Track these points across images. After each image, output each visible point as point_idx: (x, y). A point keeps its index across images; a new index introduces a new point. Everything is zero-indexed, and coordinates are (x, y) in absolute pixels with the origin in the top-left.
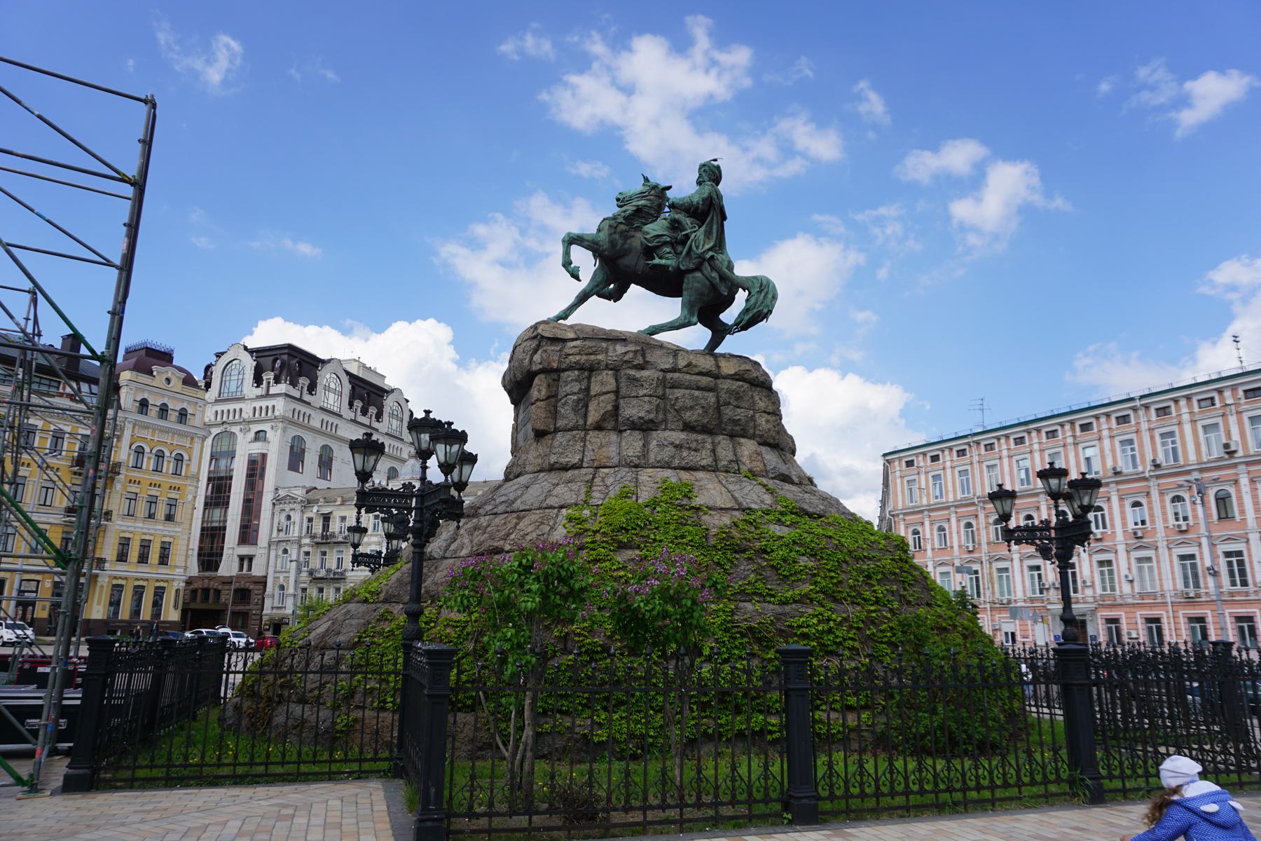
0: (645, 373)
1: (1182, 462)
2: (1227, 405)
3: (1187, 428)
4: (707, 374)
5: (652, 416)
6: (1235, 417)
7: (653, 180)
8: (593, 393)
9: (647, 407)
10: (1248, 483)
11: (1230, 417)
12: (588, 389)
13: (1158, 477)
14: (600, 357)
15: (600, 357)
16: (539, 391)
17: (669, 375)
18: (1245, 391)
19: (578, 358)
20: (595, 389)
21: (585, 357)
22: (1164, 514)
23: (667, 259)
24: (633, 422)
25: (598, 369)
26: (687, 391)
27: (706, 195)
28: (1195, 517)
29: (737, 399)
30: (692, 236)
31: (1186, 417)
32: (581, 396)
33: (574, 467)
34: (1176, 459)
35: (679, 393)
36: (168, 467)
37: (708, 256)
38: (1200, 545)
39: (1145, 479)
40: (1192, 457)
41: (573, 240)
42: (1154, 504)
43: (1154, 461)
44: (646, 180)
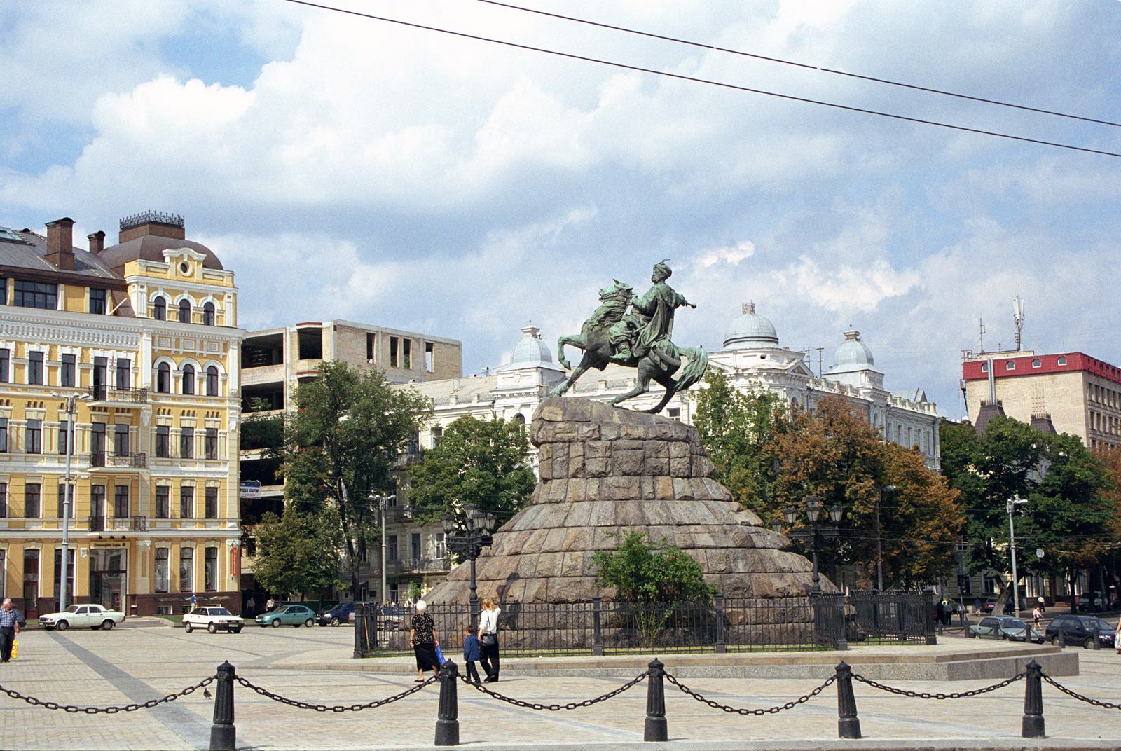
0: (599, 443)
4: (639, 438)
5: (603, 469)
9: (600, 464)
12: (568, 454)
14: (575, 434)
15: (575, 434)
17: (614, 443)
19: (562, 435)
20: (571, 455)
25: (573, 441)
26: (624, 452)
27: (650, 300)
29: (656, 453)
30: (641, 333)
32: (564, 458)
33: (561, 502)
35: (620, 453)
36: (200, 387)
37: (652, 346)
41: (564, 342)
44: (617, 282)
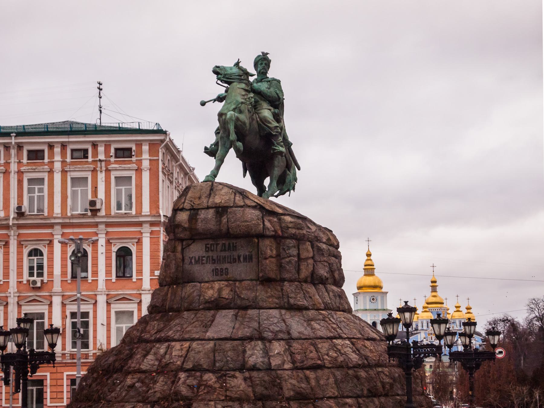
1: (46, 214)
2: (100, 161)
3: (58, 177)
4: (332, 245)
6: (104, 172)
7: (240, 65)
8: (302, 256)
10: (104, 245)
11: (99, 173)
12: (299, 255)
13: (20, 227)
15: (305, 232)
16: (271, 250)
18: (116, 150)
20: (304, 255)
21: (297, 232)
22: (20, 267)
23: (282, 147)
24: (322, 279)
25: (303, 240)
28: (51, 274)
31: (58, 166)
33: (307, 309)
34: (40, 210)
38: (50, 305)
39: (7, 227)
40: (57, 210)
42: (11, 255)
43: (19, 208)
